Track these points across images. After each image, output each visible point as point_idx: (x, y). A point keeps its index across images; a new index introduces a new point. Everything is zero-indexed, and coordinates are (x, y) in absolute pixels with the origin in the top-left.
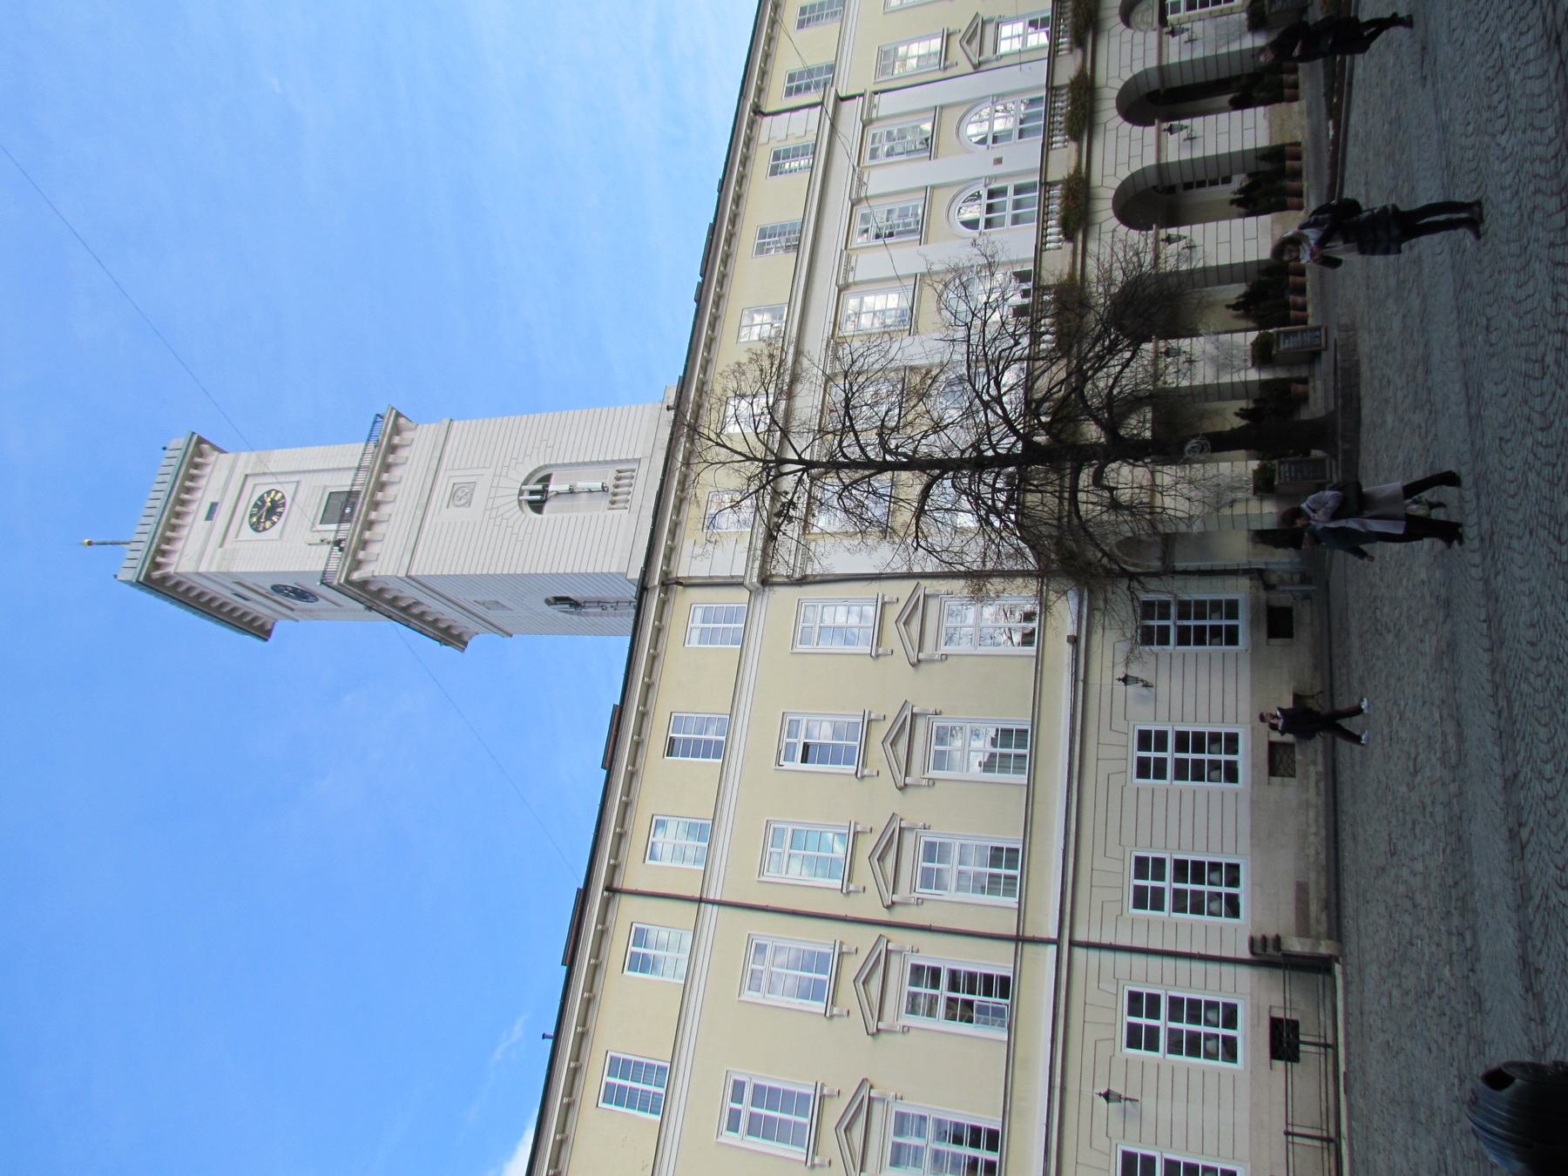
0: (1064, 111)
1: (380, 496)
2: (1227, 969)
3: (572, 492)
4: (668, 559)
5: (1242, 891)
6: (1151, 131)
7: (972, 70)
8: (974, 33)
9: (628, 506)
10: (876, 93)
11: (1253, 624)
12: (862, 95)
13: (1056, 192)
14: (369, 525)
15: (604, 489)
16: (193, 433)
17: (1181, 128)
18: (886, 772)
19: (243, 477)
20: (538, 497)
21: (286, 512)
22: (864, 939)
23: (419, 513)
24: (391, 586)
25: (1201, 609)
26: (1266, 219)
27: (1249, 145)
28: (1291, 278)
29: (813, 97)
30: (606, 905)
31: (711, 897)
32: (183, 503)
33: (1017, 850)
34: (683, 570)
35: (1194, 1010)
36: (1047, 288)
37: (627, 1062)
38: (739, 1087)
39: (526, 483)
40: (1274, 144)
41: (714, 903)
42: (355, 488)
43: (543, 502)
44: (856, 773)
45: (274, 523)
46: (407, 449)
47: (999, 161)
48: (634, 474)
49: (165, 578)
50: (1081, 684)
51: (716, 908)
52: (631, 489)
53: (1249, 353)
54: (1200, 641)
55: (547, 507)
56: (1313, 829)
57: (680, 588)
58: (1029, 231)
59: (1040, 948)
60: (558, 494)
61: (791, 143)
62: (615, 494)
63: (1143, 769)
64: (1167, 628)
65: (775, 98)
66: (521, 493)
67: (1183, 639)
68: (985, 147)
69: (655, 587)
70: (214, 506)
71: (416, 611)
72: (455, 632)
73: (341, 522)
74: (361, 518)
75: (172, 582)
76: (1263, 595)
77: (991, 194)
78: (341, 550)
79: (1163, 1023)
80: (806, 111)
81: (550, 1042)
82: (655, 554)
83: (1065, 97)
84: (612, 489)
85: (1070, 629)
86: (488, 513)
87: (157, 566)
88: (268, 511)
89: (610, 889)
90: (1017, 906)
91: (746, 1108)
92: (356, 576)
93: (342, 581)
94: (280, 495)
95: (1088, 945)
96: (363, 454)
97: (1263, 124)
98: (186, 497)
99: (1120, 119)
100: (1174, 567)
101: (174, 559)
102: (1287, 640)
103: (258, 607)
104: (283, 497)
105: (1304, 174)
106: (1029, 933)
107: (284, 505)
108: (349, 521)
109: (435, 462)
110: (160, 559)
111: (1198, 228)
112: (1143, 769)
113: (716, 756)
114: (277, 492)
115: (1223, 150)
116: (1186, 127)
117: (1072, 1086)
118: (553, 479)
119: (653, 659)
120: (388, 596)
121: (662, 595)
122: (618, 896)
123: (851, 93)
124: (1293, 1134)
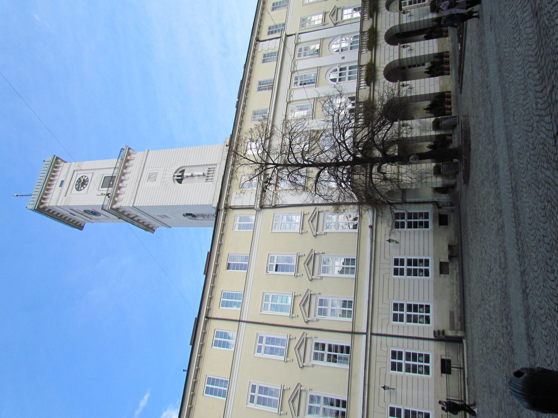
0: (366, 40)
1: (123, 178)
2: (426, 342)
3: (192, 176)
4: (227, 199)
5: (431, 315)
6: (397, 47)
7: (333, 25)
8: (334, 13)
9: (212, 181)
10: (300, 34)
11: (434, 221)
12: (295, 34)
13: (364, 69)
14: (119, 188)
15: (204, 175)
16: (55, 156)
17: (407, 46)
18: (305, 275)
19: (73, 171)
20: (180, 178)
21: (89, 184)
22: (298, 334)
23: (137, 184)
24: (127, 210)
25: (416, 216)
26: (437, 78)
27: (431, 52)
28: (446, 99)
29: (278, 35)
30: (206, 323)
31: (243, 319)
32: (51, 181)
33: (352, 301)
34: (232, 203)
35: (414, 357)
36: (361, 102)
37: (213, 379)
38: (254, 387)
39: (176, 172)
40: (439, 52)
41: (244, 322)
42: (114, 175)
43: (182, 179)
44: (295, 275)
45: (84, 188)
46: (133, 161)
47: (343, 58)
48: (215, 169)
49: (45, 208)
50: (374, 242)
51: (245, 323)
52: (213, 175)
53: (432, 125)
54: (415, 227)
55: (183, 181)
56: (455, 292)
57: (231, 209)
58: (354, 83)
59: (360, 336)
60: (187, 176)
61: (270, 51)
62: (208, 177)
63: (396, 272)
64: (404, 222)
65: (264, 35)
66: (174, 176)
67: (409, 226)
68: (338, 53)
69: (222, 209)
70: (62, 182)
71: (136, 219)
72: (151, 226)
73: (109, 187)
74: (116, 186)
75: (47, 209)
76: (437, 210)
77: (341, 70)
78: (109, 197)
79: (404, 362)
80: (275, 40)
81: (186, 372)
82: (222, 198)
83: (366, 36)
84: (206, 175)
85: (369, 222)
86: (162, 183)
87: (42, 204)
88: (82, 183)
89: (207, 317)
90: (352, 321)
92: (114, 207)
93: (109, 208)
94: (86, 177)
95: (377, 335)
96: (117, 163)
97: (436, 46)
98: (52, 178)
99: (386, 43)
100: (406, 201)
101: (48, 201)
102: (446, 226)
103: (79, 218)
104: (87, 178)
105: (450, 62)
106: (356, 331)
107: (88, 181)
108: (112, 187)
109: (143, 165)
110: (43, 201)
111: (413, 81)
112: (396, 272)
113: (245, 269)
114: (85, 177)
115: (422, 54)
116: (409, 46)
117: (372, 384)
118: (185, 171)
119: (222, 235)
120: (126, 214)
121: (225, 212)
122: (210, 320)
123: (291, 34)
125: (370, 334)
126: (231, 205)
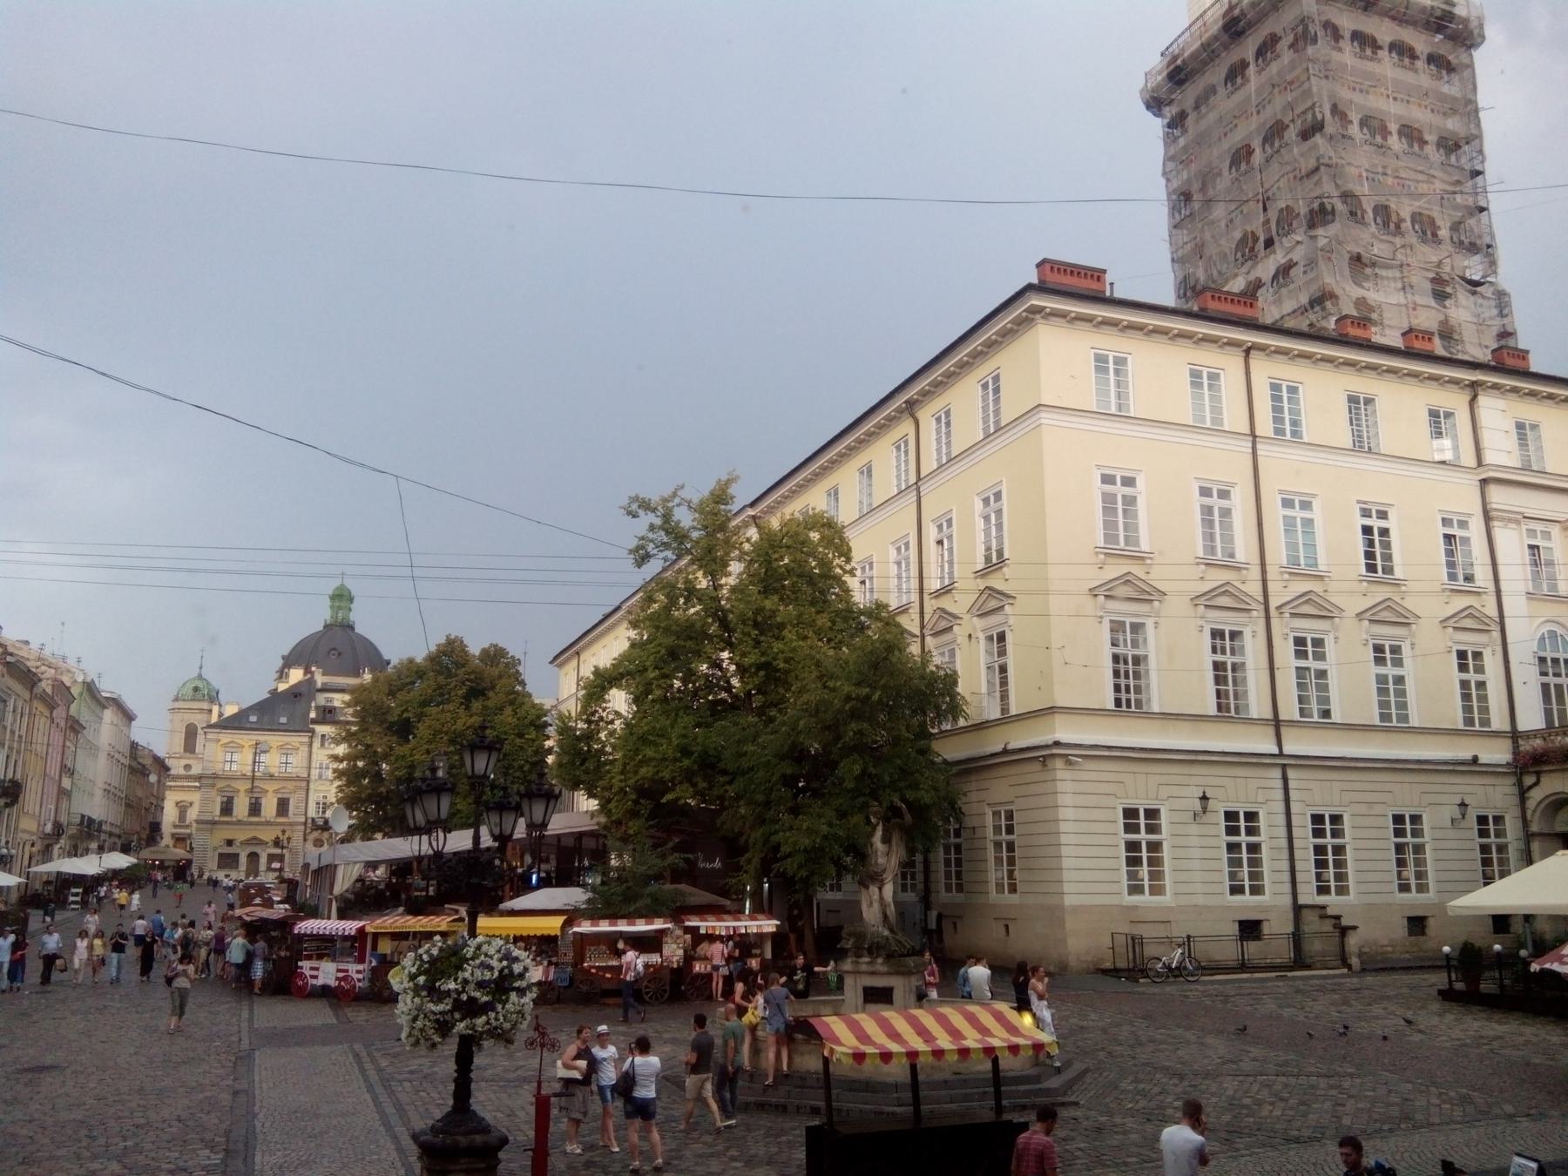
2: (1287, 888)
4: (1495, 387)
22: (1254, 588)
30: (1232, 343)
38: (1129, 482)
50: (1451, 768)
59: (1273, 740)
64: (1489, 837)
85: (1484, 758)
91: (1119, 490)
95: (1285, 779)
106: (1284, 731)
112: (1398, 819)
124: (1189, 941)
125: (1284, 763)
126: (1480, 397)
